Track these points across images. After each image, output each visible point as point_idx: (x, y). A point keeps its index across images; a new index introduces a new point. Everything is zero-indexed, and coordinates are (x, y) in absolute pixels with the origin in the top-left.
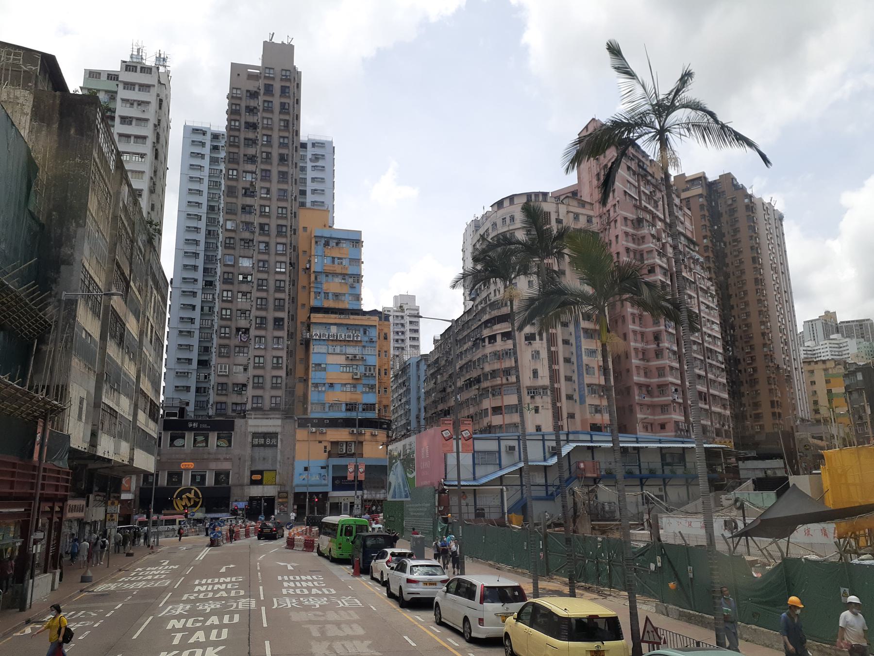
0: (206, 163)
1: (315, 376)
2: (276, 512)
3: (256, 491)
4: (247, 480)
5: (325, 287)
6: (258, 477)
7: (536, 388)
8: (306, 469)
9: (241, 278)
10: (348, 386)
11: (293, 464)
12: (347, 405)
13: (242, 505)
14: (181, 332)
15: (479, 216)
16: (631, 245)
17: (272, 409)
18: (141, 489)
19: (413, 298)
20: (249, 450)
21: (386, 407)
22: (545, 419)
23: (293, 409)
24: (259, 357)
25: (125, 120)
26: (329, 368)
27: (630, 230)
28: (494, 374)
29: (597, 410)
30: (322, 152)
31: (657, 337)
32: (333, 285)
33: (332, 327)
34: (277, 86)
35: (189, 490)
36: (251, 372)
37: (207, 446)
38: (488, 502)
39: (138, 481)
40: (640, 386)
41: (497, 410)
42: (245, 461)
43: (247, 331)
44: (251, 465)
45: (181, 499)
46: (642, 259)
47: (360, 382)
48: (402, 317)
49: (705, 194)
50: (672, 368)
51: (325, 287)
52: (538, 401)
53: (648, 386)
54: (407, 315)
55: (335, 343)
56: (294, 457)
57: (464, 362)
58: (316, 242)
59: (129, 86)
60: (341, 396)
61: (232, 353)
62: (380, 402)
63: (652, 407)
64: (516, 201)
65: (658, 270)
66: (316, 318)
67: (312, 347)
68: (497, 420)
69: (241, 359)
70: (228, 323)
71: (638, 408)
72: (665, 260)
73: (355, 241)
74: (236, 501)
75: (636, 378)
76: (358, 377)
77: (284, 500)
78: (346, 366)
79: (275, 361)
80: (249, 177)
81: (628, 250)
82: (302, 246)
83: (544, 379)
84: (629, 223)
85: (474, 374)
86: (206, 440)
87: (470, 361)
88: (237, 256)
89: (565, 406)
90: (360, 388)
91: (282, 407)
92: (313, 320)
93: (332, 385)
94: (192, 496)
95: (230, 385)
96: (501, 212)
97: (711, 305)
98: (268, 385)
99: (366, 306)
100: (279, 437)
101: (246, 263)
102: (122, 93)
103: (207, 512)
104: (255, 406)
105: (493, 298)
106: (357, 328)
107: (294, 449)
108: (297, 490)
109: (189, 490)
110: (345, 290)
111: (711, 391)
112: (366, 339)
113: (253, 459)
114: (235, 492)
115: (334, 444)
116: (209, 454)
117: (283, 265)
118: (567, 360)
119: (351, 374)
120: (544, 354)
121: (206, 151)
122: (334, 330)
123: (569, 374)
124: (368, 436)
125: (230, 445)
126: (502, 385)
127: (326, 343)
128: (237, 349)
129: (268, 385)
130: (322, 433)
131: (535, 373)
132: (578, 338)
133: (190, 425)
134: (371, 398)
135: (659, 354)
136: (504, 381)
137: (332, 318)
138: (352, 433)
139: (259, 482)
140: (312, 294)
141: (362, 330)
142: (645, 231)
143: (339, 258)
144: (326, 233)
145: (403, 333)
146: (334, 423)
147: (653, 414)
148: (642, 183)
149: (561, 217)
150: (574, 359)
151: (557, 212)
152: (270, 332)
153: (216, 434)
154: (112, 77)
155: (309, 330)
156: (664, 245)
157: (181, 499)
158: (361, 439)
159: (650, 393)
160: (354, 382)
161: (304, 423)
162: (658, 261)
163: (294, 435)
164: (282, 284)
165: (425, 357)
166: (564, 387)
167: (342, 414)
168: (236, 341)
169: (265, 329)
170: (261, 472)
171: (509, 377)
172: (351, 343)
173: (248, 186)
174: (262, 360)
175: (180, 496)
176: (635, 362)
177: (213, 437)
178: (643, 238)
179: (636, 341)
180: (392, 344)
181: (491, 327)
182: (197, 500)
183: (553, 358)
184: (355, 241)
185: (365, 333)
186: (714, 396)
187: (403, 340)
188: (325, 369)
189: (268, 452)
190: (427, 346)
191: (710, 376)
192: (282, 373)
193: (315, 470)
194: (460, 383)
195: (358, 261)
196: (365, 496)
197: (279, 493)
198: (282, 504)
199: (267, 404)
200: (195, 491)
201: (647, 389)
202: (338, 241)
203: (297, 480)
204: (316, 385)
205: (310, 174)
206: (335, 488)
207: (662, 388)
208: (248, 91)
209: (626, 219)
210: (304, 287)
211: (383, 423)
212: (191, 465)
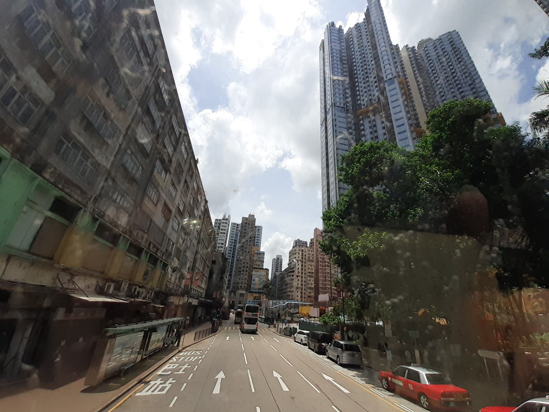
0: (235, 231)
1: (253, 282)
3: (239, 305)
22: (299, 294)
23: (248, 289)
25: (222, 230)
29: (310, 293)
30: (260, 229)
31: (325, 277)
34: (251, 223)
36: (241, 281)
38: (274, 310)
41: (290, 291)
59: (223, 223)
60: (257, 287)
69: (239, 277)
73: (263, 253)
83: (300, 286)
89: (303, 291)
99: (264, 268)
101: (241, 257)
102: (222, 224)
120: (300, 280)
121: (235, 228)
135: (326, 281)
144: (258, 252)
152: (245, 273)
154: (220, 220)
159: (323, 289)
161: (249, 292)
167: (257, 291)
183: (302, 281)
184: (263, 253)
201: (323, 288)
202: (260, 254)
205: (257, 233)
207: (326, 288)
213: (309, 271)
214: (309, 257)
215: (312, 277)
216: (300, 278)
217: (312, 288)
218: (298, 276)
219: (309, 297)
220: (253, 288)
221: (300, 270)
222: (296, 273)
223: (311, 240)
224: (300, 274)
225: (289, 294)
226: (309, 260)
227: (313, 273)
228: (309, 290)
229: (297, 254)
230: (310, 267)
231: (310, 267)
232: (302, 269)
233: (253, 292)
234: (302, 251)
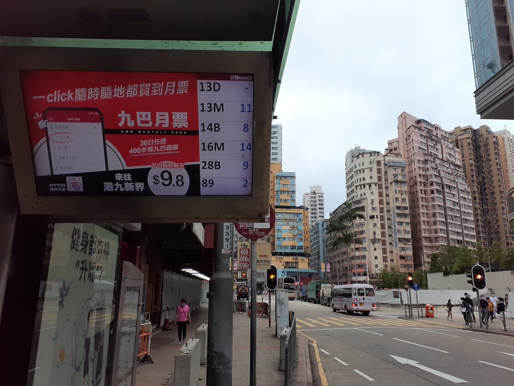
15: (354, 149)
16: (422, 173)
19: (320, 187)
21: (307, 247)
22: (379, 253)
27: (421, 165)
29: (403, 249)
32: (284, 197)
40: (426, 238)
41: (357, 249)
46: (427, 179)
48: (315, 197)
49: (471, 137)
50: (441, 230)
52: (377, 245)
53: (429, 238)
54: (316, 197)
60: (288, 243)
62: (305, 246)
63: (431, 247)
64: (365, 155)
65: (434, 184)
66: (277, 210)
68: (357, 254)
71: (424, 248)
72: (439, 178)
75: (423, 235)
81: (420, 175)
83: (379, 236)
84: (421, 162)
89: (388, 247)
90: (296, 240)
93: (284, 238)
96: (358, 160)
97: (467, 197)
110: (289, 198)
111: (465, 239)
115: (287, 263)
118: (390, 227)
120: (379, 225)
123: (390, 233)
124: (300, 260)
130: (282, 258)
131: (374, 233)
132: (394, 217)
134: (301, 244)
135: (435, 223)
137: (284, 210)
140: (275, 201)
142: (429, 166)
145: (315, 205)
146: (286, 254)
147: (433, 251)
148: (429, 141)
149: (386, 163)
150: (393, 227)
151: (384, 160)
156: (439, 171)
162: (435, 180)
165: (326, 221)
166: (387, 239)
167: (289, 251)
176: (423, 227)
178: (428, 169)
179: (424, 217)
180: (310, 219)
183: (383, 226)
186: (467, 242)
187: (315, 209)
188: (281, 232)
190: (327, 217)
191: (465, 232)
201: (429, 239)
202: (285, 177)
204: (279, 238)
209: (419, 160)
211: (306, 255)
213: (399, 204)
214: (395, 175)
215: (405, 216)
217: (407, 240)
219: (402, 257)
220: (281, 247)
221: (377, 205)
222: (368, 212)
223: (390, 143)
224: (377, 213)
226: (397, 182)
227: (406, 208)
228: (400, 245)
229: (367, 171)
230: (398, 195)
231: (398, 195)
232: (381, 202)
233: (281, 254)
234: (379, 163)
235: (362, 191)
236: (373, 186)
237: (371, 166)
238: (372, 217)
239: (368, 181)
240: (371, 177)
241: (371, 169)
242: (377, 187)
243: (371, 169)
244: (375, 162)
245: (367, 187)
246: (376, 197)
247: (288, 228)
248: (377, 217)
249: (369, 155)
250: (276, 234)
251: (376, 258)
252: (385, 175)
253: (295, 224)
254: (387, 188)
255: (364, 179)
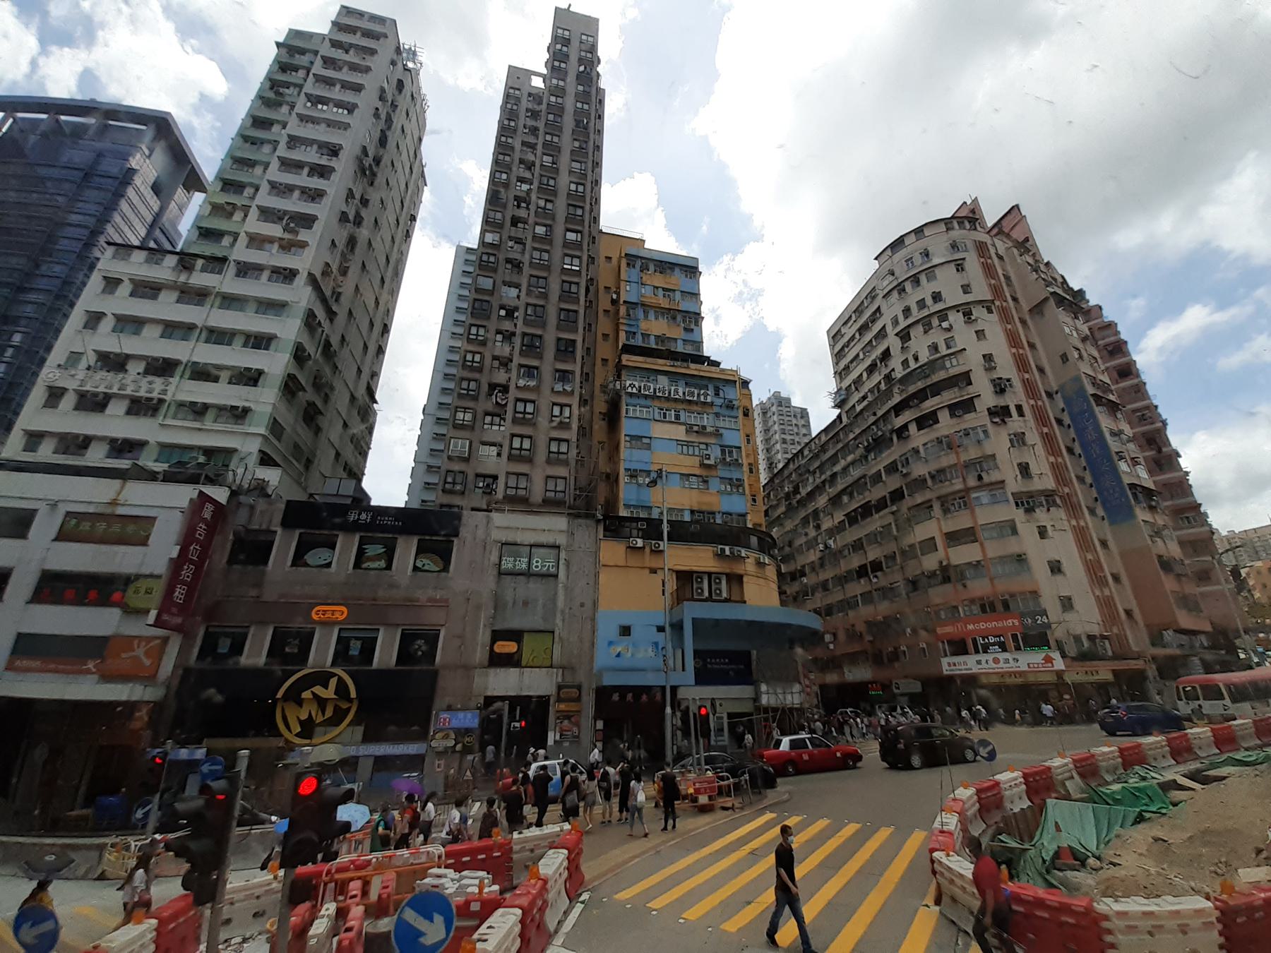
1: (629, 457)
2: (551, 738)
3: (504, 682)
4: (480, 655)
5: (643, 325)
6: (511, 647)
7: (1031, 495)
8: (626, 631)
9: (503, 313)
10: (693, 479)
11: (593, 619)
12: (692, 512)
13: (469, 720)
14: (429, 466)
17: (546, 502)
18: (187, 671)
20: (489, 581)
24: (525, 401)
26: (654, 444)
28: (938, 476)
33: (660, 378)
35: (322, 678)
37: (389, 567)
39: (184, 651)
41: (953, 538)
42: (478, 607)
43: (505, 389)
44: (494, 617)
45: (300, 703)
47: (714, 473)
51: (643, 325)
55: (665, 405)
56: (595, 604)
57: (840, 487)
58: (628, 265)
61: (478, 424)
64: (927, 232)
67: (624, 408)
68: (963, 555)
70: (477, 376)
74: (449, 708)
76: (711, 462)
77: (573, 707)
78: (688, 444)
79: (556, 411)
80: (525, 187)
82: (605, 279)
85: (875, 494)
86: (389, 556)
87: (864, 476)
88: (499, 282)
90: (715, 485)
91: (569, 499)
92: (624, 362)
94: (329, 693)
95: (471, 477)
96: (902, 254)
98: (541, 456)
100: (563, 555)
103: (367, 739)
104: (511, 492)
105: (899, 374)
106: (705, 382)
107: (596, 583)
108: (608, 680)
109: (322, 678)
112: (718, 401)
113: (498, 603)
114: (449, 685)
115: (685, 577)
116: (392, 586)
117: (576, 261)
119: (696, 461)
120: (1033, 437)
122: (663, 381)
124: (750, 565)
125: (446, 569)
126: (968, 490)
127: (648, 402)
128: (488, 419)
129: (541, 456)
131: (1024, 469)
133: (352, 517)
136: (972, 482)
137: (660, 364)
138: (720, 556)
139: (510, 661)
141: (711, 387)
143: (664, 289)
153: (414, 541)
155: (619, 376)
157: (300, 703)
158: (739, 569)
160: (704, 473)
161: (614, 526)
163: (596, 554)
164: (574, 288)
168: (489, 406)
169: (540, 357)
170: (516, 635)
171: (984, 475)
172: (695, 408)
173: (523, 195)
174: (530, 408)
175: (294, 696)
177: (406, 550)
181: (917, 405)
182: (344, 706)
185: (717, 394)
188: (648, 447)
189: (535, 588)
192: (572, 435)
193: (644, 633)
194: (827, 524)
195: (695, 295)
196: (764, 700)
197: (560, 687)
198: (567, 716)
199: (537, 495)
200: (341, 684)
203: (603, 657)
204: (633, 474)
206: (702, 678)
208: (530, 95)
210: (605, 336)
212: (341, 613)
216: (1025, 425)
218: (1000, 414)
221: (1006, 368)
225: (963, 555)
233: (652, 530)
234: (981, 248)
235: (937, 337)
236: (978, 312)
237: (957, 256)
238: (1000, 414)
239: (954, 296)
240: (966, 289)
241: (960, 267)
242: (994, 317)
243: (960, 267)
244: (970, 245)
245: (956, 318)
246: (997, 343)
247: (679, 432)
248: (1021, 414)
249: (943, 227)
250: (624, 453)
251: (1056, 568)
252: (1008, 285)
253: (707, 421)
254: (1023, 322)
255: (937, 297)
